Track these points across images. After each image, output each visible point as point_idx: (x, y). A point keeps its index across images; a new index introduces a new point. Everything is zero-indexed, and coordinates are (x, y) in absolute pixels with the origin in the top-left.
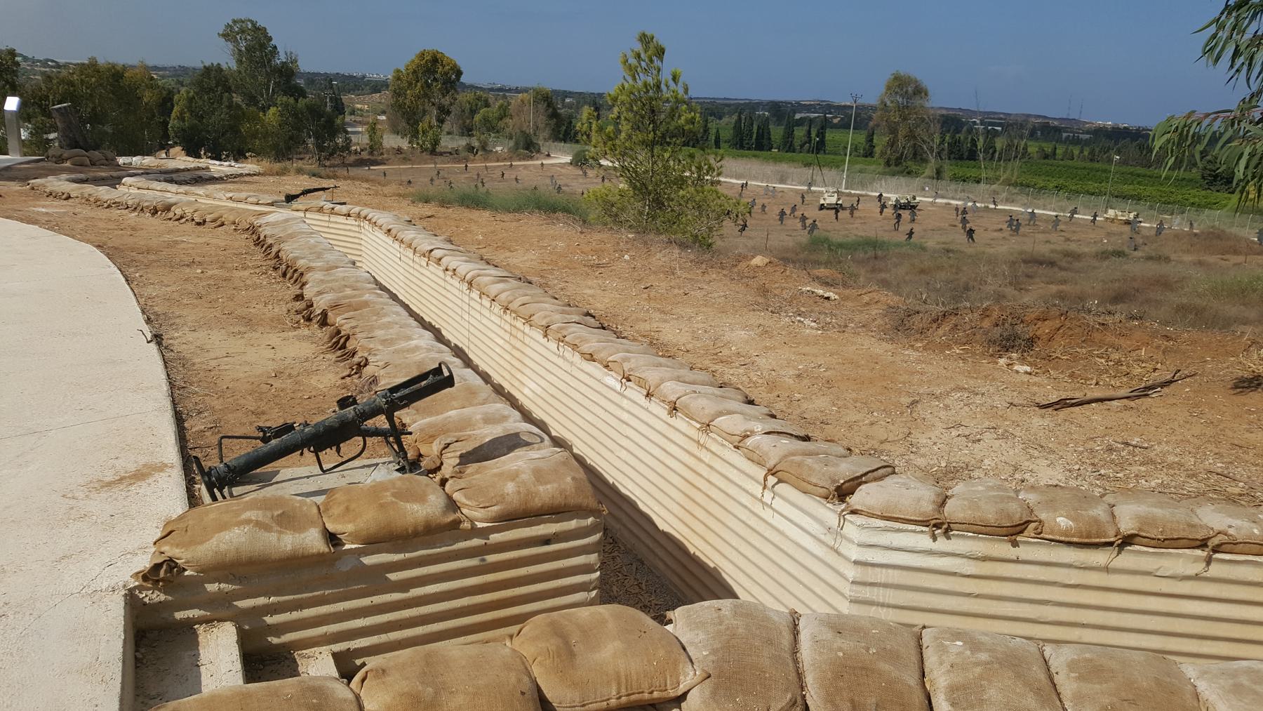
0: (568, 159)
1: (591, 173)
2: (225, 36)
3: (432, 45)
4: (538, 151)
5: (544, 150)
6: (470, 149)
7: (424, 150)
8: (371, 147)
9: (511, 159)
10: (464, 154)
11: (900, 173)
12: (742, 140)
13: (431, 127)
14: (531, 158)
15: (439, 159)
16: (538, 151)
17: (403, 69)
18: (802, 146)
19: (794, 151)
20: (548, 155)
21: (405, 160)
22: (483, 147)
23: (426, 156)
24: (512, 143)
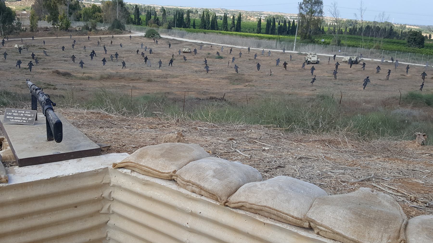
0: (143, 34)
1: (159, 42)
5: (127, 29)
6: (87, 28)
7: (62, 29)
8: (32, 27)
9: (110, 34)
10: (85, 31)
11: (308, 43)
12: (205, 25)
13: (65, 17)
14: (121, 33)
16: (124, 30)
18: (231, 28)
19: (228, 31)
20: (130, 32)
21: (51, 34)
22: (94, 27)
23: (63, 32)
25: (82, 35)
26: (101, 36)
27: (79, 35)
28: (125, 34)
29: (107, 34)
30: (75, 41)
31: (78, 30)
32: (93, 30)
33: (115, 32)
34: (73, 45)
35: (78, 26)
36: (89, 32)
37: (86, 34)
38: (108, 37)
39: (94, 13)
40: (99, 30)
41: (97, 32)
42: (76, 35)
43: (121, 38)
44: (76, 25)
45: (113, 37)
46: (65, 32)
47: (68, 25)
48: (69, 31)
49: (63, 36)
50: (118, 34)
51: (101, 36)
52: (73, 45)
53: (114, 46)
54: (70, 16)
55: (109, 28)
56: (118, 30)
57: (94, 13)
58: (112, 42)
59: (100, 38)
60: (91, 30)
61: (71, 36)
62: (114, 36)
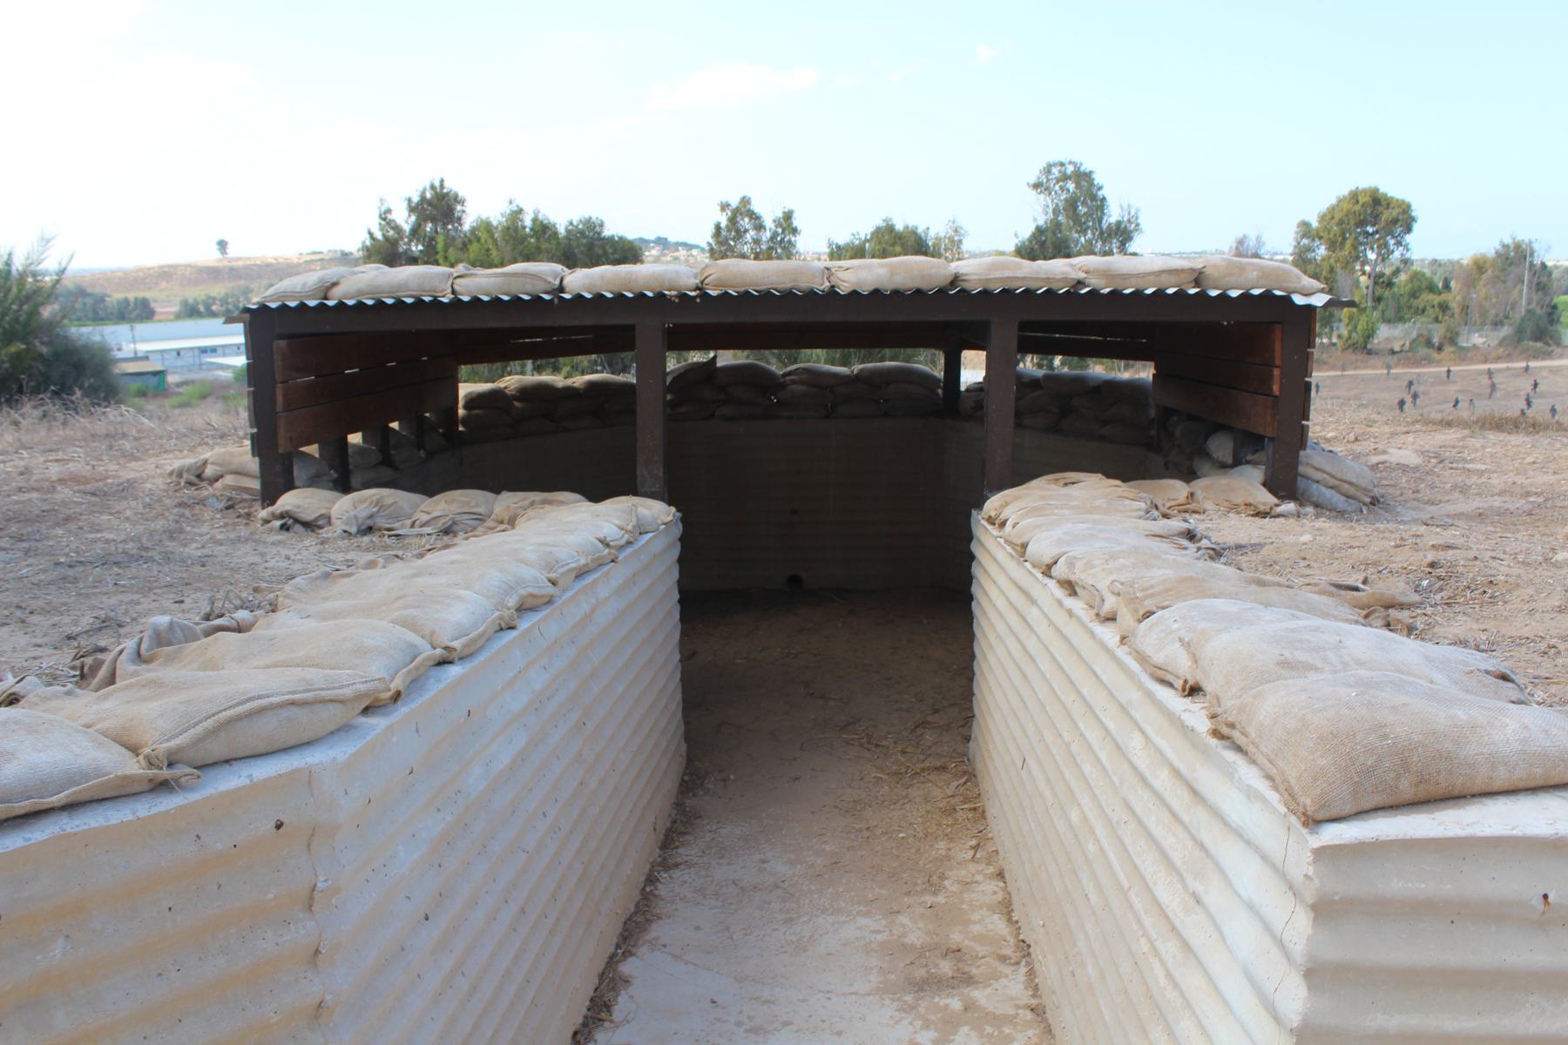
2: (1036, 186)
3: (1364, 183)
4: (1558, 344)
9: (1509, 357)
10: (1423, 351)
14: (1548, 355)
15: (1374, 360)
17: (1315, 224)
22: (1452, 339)
24: (1505, 331)
25: (1417, 363)
26: (1493, 366)
27: (1404, 366)
28: (1561, 357)
29: (1498, 359)
30: (1411, 383)
31: (1397, 348)
32: (1448, 349)
33: (1524, 351)
34: (1415, 396)
35: (1388, 339)
36: (1435, 355)
37: (1429, 361)
38: (1508, 369)
39: (1414, 294)
40: (1463, 348)
41: (1464, 355)
42: (1396, 366)
43: (1554, 371)
44: (1384, 332)
45: (1527, 369)
46: (1360, 357)
47: (1370, 335)
48: (1370, 353)
49: (1356, 368)
50: (1536, 358)
51: (1493, 366)
52: (1415, 396)
53: (1543, 396)
54: (1375, 308)
55: (1504, 339)
56: (1539, 344)
57: (1414, 294)
58: (1536, 385)
59: (1490, 373)
60: (1440, 349)
61: (1389, 367)
62: (1532, 364)
